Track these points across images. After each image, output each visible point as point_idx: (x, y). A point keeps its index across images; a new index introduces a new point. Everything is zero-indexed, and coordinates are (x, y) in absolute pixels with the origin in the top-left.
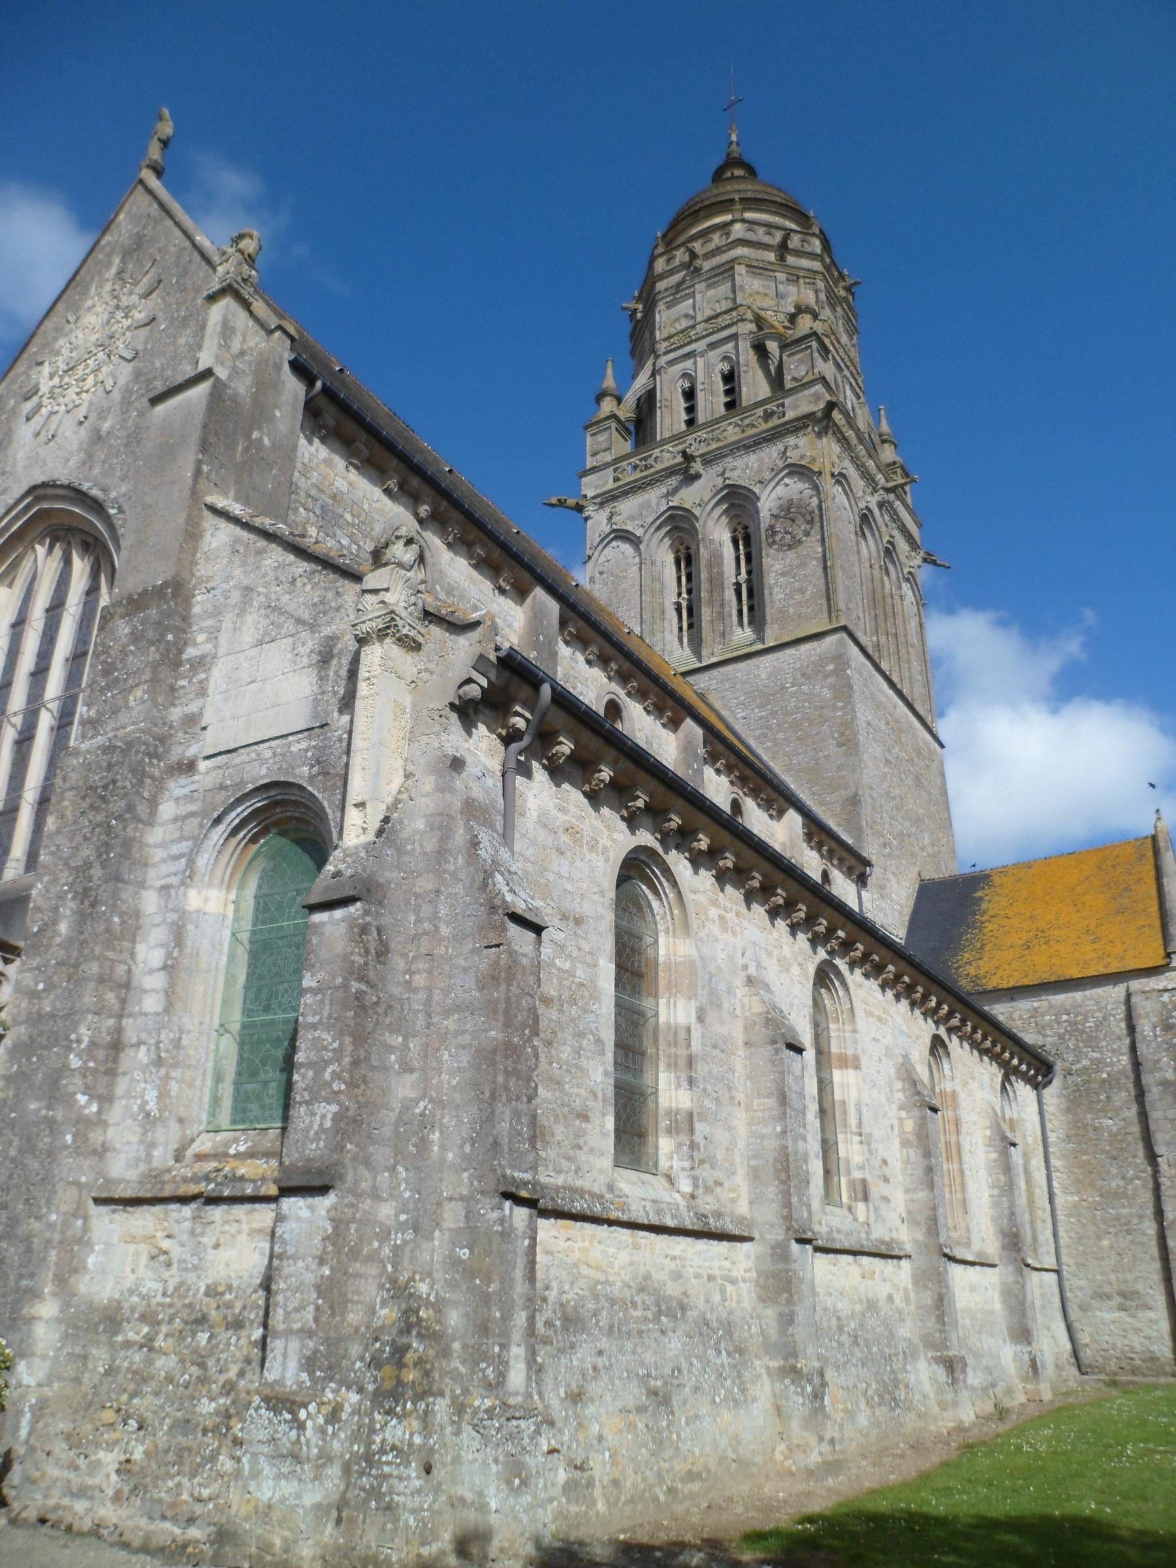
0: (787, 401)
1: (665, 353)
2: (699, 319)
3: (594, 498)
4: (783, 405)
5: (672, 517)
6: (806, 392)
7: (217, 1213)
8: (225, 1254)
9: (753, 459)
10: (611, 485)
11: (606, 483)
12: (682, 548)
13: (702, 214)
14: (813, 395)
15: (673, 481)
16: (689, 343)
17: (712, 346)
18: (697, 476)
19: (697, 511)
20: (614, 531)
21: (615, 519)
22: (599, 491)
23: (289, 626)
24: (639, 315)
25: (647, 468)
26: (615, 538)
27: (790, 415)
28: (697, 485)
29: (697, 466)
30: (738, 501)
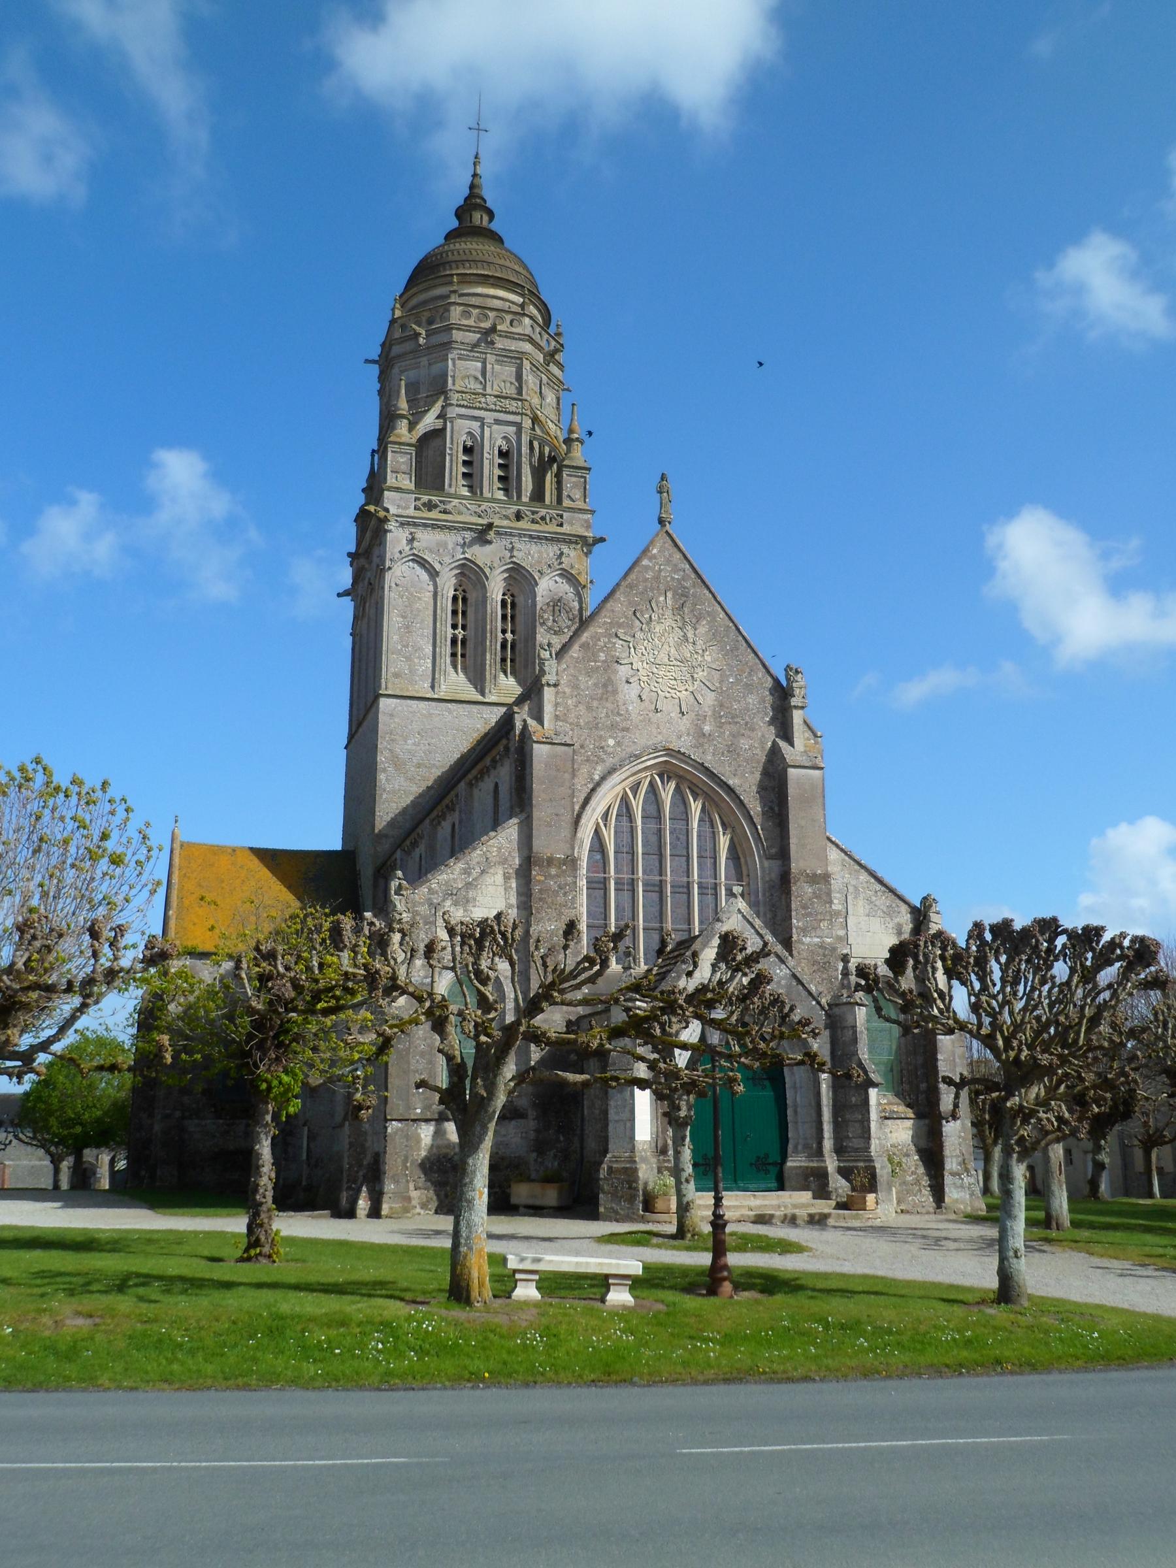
0: (565, 515)
1: (459, 406)
2: (489, 391)
4: (561, 516)
5: (463, 565)
7: (889, 1122)
8: (894, 1135)
9: (534, 548)
10: (411, 511)
11: (407, 508)
14: (587, 521)
15: (469, 535)
16: (479, 409)
17: (498, 422)
18: (490, 542)
19: (487, 571)
20: (414, 555)
21: (416, 544)
22: (400, 512)
23: (880, 913)
24: (421, 341)
25: (445, 512)
27: (566, 529)
28: (488, 548)
29: (491, 535)
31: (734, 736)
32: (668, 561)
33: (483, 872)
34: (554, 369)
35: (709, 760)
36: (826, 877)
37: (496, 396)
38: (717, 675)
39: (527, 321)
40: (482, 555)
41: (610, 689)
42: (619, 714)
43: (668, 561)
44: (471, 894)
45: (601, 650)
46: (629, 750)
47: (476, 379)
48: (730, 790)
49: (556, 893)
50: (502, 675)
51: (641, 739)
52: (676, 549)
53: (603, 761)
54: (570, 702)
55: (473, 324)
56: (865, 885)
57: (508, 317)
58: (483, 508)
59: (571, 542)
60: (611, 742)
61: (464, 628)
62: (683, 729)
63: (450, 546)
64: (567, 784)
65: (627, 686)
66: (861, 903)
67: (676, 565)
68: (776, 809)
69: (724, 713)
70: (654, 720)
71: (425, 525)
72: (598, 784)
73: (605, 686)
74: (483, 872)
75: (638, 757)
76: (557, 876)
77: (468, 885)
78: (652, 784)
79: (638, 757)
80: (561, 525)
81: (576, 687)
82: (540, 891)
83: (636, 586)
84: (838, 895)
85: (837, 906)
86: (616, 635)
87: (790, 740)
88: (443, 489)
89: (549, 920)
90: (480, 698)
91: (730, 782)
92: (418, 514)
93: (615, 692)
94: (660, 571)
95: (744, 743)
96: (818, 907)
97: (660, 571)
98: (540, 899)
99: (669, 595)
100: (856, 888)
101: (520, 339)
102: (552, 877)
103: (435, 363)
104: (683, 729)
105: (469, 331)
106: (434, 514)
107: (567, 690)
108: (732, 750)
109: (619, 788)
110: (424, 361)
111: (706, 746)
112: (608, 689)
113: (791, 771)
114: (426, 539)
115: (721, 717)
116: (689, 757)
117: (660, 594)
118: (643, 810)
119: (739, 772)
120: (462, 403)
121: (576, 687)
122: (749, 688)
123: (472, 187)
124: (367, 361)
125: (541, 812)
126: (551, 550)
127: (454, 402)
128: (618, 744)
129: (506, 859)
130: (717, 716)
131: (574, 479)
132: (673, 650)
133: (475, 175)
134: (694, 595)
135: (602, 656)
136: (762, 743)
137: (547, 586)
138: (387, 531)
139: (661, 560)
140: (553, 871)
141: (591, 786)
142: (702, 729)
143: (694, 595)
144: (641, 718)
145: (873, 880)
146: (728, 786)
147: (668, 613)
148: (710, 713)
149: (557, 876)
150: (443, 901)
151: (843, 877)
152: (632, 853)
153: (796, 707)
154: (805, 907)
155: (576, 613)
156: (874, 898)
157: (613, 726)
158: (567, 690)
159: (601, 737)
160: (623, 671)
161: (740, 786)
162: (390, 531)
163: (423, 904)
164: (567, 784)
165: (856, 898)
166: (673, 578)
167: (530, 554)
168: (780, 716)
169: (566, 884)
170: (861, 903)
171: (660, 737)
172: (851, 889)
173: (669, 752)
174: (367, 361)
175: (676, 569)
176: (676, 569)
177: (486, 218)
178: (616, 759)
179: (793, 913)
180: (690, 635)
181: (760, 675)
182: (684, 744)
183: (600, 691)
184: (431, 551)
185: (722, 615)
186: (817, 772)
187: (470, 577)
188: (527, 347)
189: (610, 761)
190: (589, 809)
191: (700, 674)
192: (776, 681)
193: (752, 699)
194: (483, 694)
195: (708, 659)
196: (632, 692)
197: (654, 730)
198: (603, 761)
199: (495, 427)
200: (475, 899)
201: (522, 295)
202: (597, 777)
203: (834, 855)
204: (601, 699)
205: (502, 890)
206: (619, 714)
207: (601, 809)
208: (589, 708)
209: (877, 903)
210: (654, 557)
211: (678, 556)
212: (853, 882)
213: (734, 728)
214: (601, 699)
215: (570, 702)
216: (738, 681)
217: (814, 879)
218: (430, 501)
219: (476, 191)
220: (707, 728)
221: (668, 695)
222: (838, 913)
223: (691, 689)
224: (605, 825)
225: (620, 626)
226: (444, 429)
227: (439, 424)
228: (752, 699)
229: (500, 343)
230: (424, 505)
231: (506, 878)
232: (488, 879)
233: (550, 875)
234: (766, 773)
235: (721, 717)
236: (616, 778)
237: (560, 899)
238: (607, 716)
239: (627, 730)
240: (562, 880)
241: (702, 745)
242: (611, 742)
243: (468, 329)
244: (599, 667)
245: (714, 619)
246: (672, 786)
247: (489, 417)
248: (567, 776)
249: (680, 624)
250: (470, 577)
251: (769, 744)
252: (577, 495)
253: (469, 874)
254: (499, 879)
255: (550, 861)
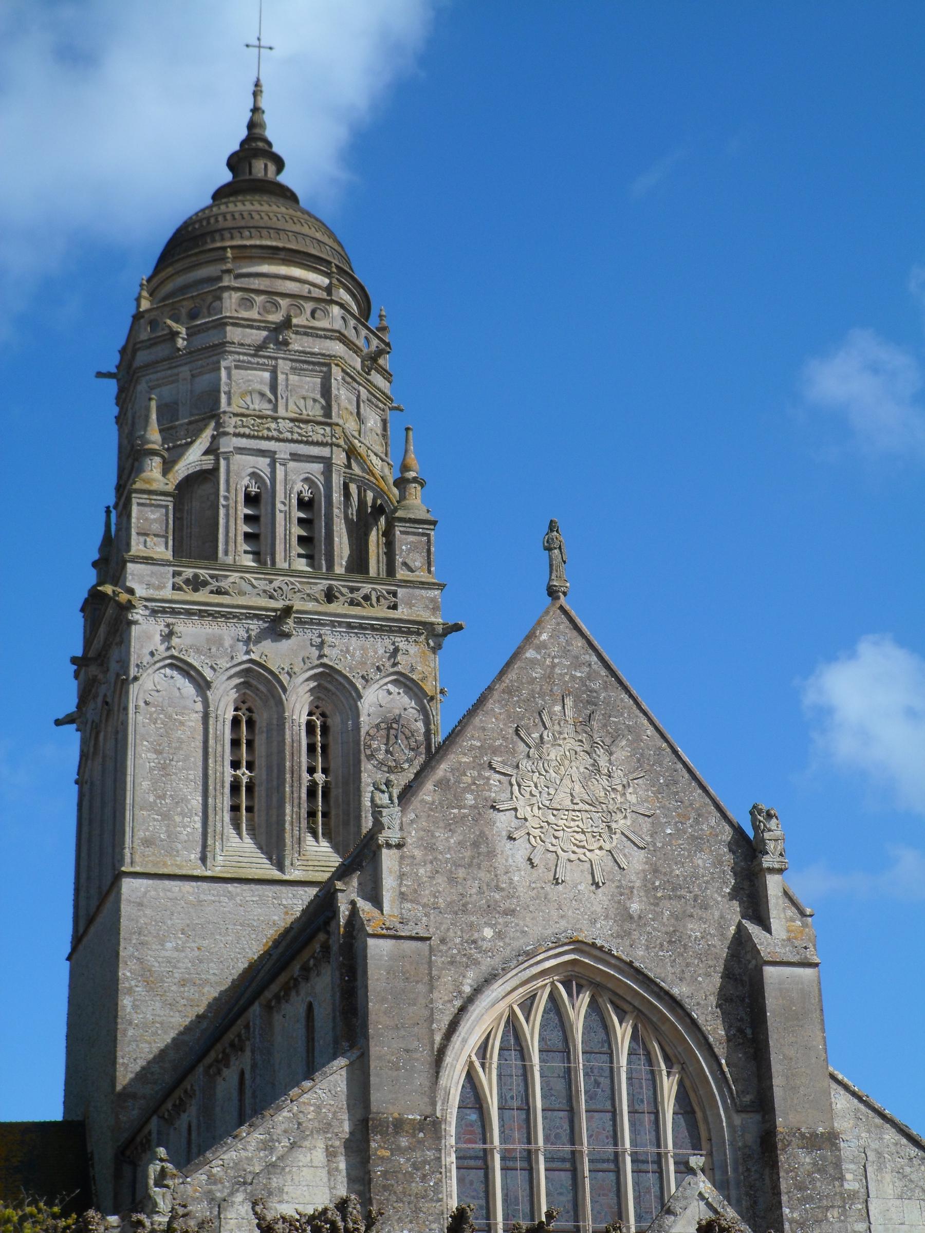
0: (401, 592)
1: (237, 435)
2: (281, 412)
3: (147, 600)
4: (395, 594)
5: (247, 670)
6: (423, 592)
9: (355, 642)
10: (167, 593)
11: (161, 587)
12: (244, 707)
13: (282, 255)
14: (433, 600)
15: (255, 626)
16: (268, 439)
17: (295, 457)
18: (288, 636)
19: (284, 678)
20: (172, 657)
21: (175, 641)
22: (151, 593)
24: (181, 343)
25: (219, 592)
26: (170, 666)
27: (402, 612)
28: (285, 644)
29: (289, 624)
30: (333, 689)
31: (677, 919)
32: (565, 652)
33: (293, 1146)
34: (377, 379)
35: (640, 957)
36: (832, 1139)
37: (292, 420)
38: (646, 824)
39: (336, 310)
40: (275, 654)
41: (483, 849)
42: (498, 888)
43: (565, 652)
44: (275, 1182)
45: (468, 789)
46: (516, 944)
47: (262, 395)
48: (675, 1003)
49: (409, 1177)
50: (309, 839)
51: (535, 927)
52: (575, 633)
53: (477, 963)
54: (422, 871)
55: (257, 317)
56: (893, 1149)
57: (309, 306)
58: (276, 584)
59: (409, 632)
60: (488, 933)
61: (250, 766)
62: (598, 909)
63: (227, 643)
64: (422, 1001)
65: (509, 845)
66: (888, 1178)
67: (577, 657)
68: (749, 1031)
69: (661, 883)
70: (553, 896)
71: (189, 613)
72: (470, 1000)
73: (476, 845)
74: (293, 1146)
75: (530, 955)
76: (411, 1149)
77: (271, 1168)
78: (553, 998)
79: (530, 955)
80: (395, 607)
81: (430, 848)
82: (385, 1174)
83: (518, 689)
84: (852, 1166)
85: (851, 1183)
86: (490, 766)
87: (764, 923)
88: (214, 556)
89: (400, 1220)
90: (276, 874)
91: (675, 991)
92: (179, 596)
93: (491, 854)
94: (553, 666)
95: (693, 929)
96: (822, 1186)
97: (553, 666)
98: (385, 1188)
99: (569, 702)
100: (879, 1154)
101: (326, 337)
102: (399, 1150)
103: (201, 374)
104: (598, 909)
105: (251, 327)
106: (202, 596)
107: (418, 853)
108: (675, 939)
109: (503, 1006)
110: (185, 371)
111: (635, 935)
112: (481, 849)
113: (768, 970)
114: (191, 632)
115: (656, 889)
116: (609, 953)
117: (554, 702)
118: (542, 1039)
119: (687, 975)
120: (242, 430)
121: (430, 848)
122: (697, 842)
123: (251, 125)
124: (99, 375)
125: (383, 1046)
126: (379, 646)
127: (231, 430)
128: (499, 935)
129: (329, 1124)
130: (649, 889)
131: (411, 538)
132: (578, 788)
133: (256, 110)
134: (607, 703)
135: (470, 799)
136: (722, 928)
137: (377, 700)
138: (131, 623)
139: (554, 650)
140: (404, 1142)
141: (458, 1003)
142: (627, 909)
143: (607, 703)
144: (533, 894)
145: (904, 1141)
146: (672, 998)
147: (569, 729)
148: (638, 884)
149: (411, 1149)
150: (232, 1194)
151: (858, 1138)
152: (527, 1108)
153: (771, 870)
154: (801, 1187)
155: (421, 738)
156: (908, 1170)
157: (490, 908)
158: (418, 853)
159: (471, 925)
160: (503, 821)
161: (691, 997)
162: (136, 623)
163: (199, 1200)
164: (422, 1001)
165: (880, 1169)
166: (573, 677)
167: (350, 652)
168: (746, 884)
169: (425, 1162)
170: (888, 1178)
171: (563, 923)
172: (872, 1156)
173: (579, 946)
174: (99, 375)
175: (577, 664)
176: (577, 664)
177: (272, 168)
178: (497, 959)
179: (784, 1198)
180: (603, 763)
181: (713, 822)
182: (601, 933)
183: (468, 854)
184: (198, 651)
185: (650, 731)
186: (808, 971)
187: (259, 686)
188: (338, 348)
189: (487, 964)
190: (457, 1040)
191: (621, 823)
192: (738, 831)
193: (702, 860)
194: (281, 867)
195: (632, 799)
196: (517, 853)
197: (555, 914)
198: (477, 963)
199: (292, 465)
200: (281, 1190)
201: (328, 275)
202: (467, 989)
203: (841, 1102)
204: (470, 865)
205: (323, 1173)
206: (498, 888)
207: (475, 1040)
208: (452, 880)
209: (914, 1177)
210: (544, 645)
211: (580, 643)
212: (875, 1145)
213: (677, 905)
214: (470, 865)
215: (422, 871)
216: (679, 832)
217: (813, 1142)
218: (196, 576)
219: (257, 131)
220: (635, 907)
221: (573, 857)
222: (853, 1196)
223: (607, 846)
224: (483, 1066)
225: (495, 751)
226: (216, 469)
227: (208, 463)
228: (702, 860)
229: (297, 343)
230: (187, 582)
231: (331, 1154)
232: (302, 1157)
233: (399, 1148)
234: (728, 975)
235: (656, 889)
236: (497, 990)
237: (417, 1186)
238: (480, 892)
239: (511, 912)
240: (417, 1155)
241: (628, 934)
242: (488, 933)
243: (250, 324)
244: (465, 816)
245: (638, 739)
246: (585, 999)
247: (283, 450)
248: (421, 988)
249: (587, 747)
250: (259, 686)
251: (733, 929)
252: (417, 561)
253: (272, 1149)
254: (319, 1156)
255: (399, 1125)
